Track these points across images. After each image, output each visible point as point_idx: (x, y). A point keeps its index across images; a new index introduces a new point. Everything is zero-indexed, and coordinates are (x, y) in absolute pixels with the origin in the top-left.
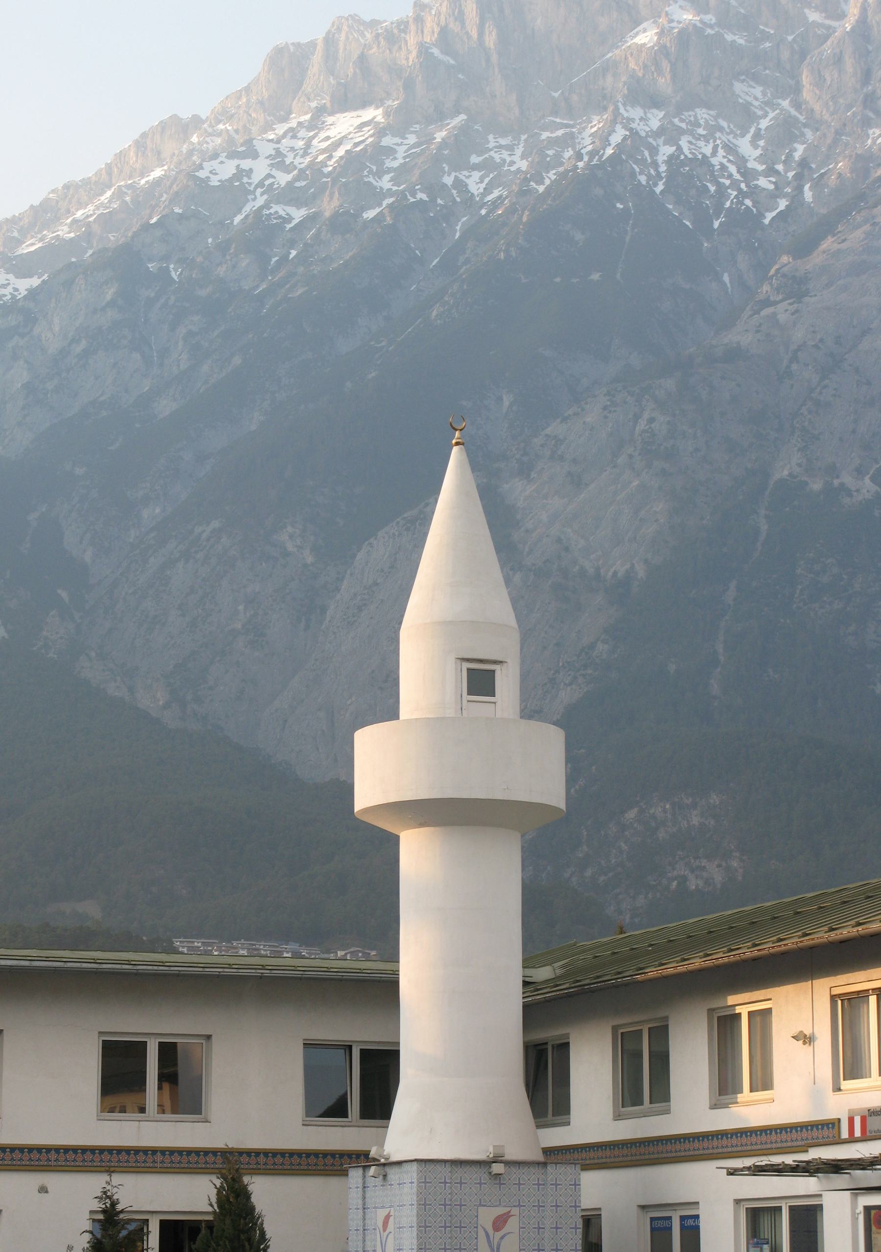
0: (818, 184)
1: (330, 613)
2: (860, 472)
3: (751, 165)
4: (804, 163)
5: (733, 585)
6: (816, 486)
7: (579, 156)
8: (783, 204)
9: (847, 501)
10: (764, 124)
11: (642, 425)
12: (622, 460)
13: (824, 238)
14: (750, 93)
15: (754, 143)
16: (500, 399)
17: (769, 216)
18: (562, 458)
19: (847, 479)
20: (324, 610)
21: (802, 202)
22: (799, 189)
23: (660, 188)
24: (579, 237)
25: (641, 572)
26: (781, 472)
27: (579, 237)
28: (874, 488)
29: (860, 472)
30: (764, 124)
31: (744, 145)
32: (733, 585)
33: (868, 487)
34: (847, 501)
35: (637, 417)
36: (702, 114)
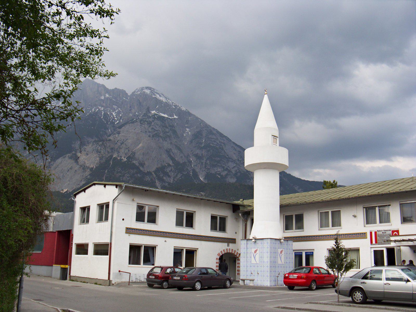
0: (123, 120)
1: (52, 168)
2: (125, 157)
3: (114, 116)
4: (121, 117)
5: (107, 170)
6: (119, 158)
7: (92, 112)
8: (118, 122)
9: (122, 161)
10: (116, 111)
11: (97, 148)
12: (94, 152)
13: (123, 126)
14: (115, 107)
15: (115, 113)
16: (78, 142)
17: (116, 123)
18: (86, 151)
19: (123, 158)
20: (51, 168)
21: (120, 122)
22: (120, 120)
23: (102, 117)
24: (91, 122)
25: (95, 167)
26: (114, 156)
27: (91, 122)
28: (126, 160)
29: (125, 157)
30: (116, 111)
31: (114, 113)
32: (107, 170)
33: (125, 160)
34: (122, 161)
35: (96, 147)
36: (109, 109)
